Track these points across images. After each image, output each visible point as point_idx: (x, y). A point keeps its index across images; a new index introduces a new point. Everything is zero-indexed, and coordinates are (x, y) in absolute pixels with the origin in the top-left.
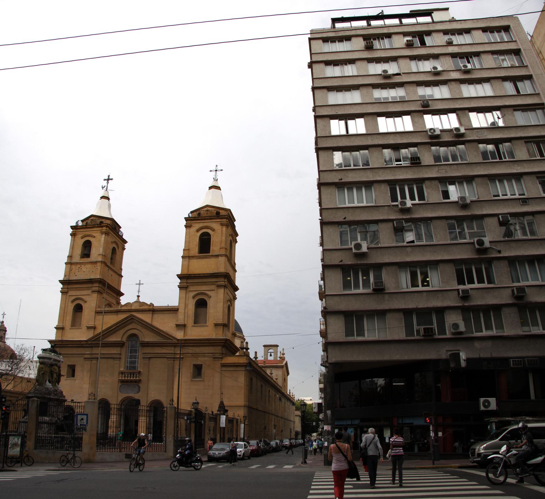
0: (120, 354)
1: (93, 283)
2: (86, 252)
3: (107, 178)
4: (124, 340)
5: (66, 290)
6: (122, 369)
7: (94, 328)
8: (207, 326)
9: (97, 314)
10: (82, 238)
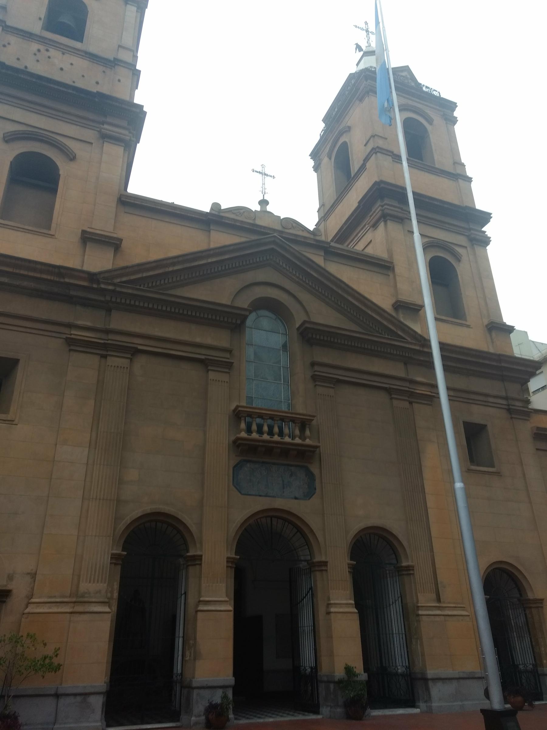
0: (230, 351)
8: (468, 326)
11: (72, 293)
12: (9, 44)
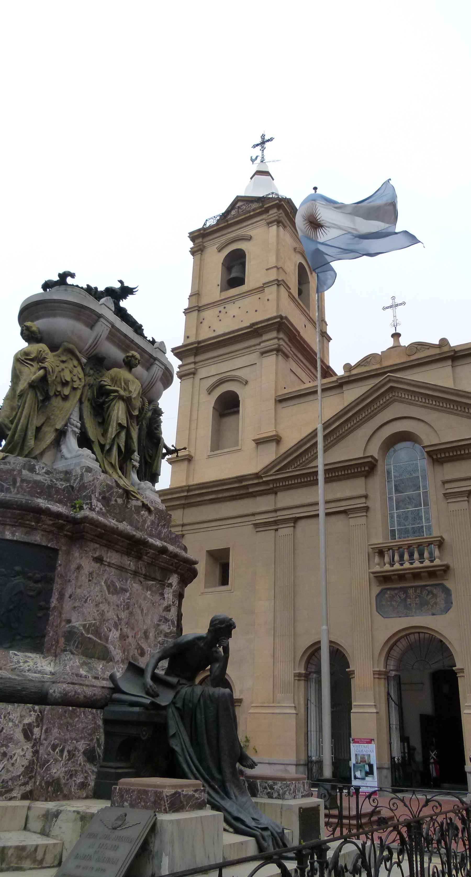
0: (366, 497)
1: (260, 335)
2: (234, 274)
3: (259, 141)
4: (374, 450)
5: (192, 366)
6: (379, 539)
7: (277, 440)
9: (280, 406)
10: (220, 250)
11: (251, 490)
12: (203, 319)
